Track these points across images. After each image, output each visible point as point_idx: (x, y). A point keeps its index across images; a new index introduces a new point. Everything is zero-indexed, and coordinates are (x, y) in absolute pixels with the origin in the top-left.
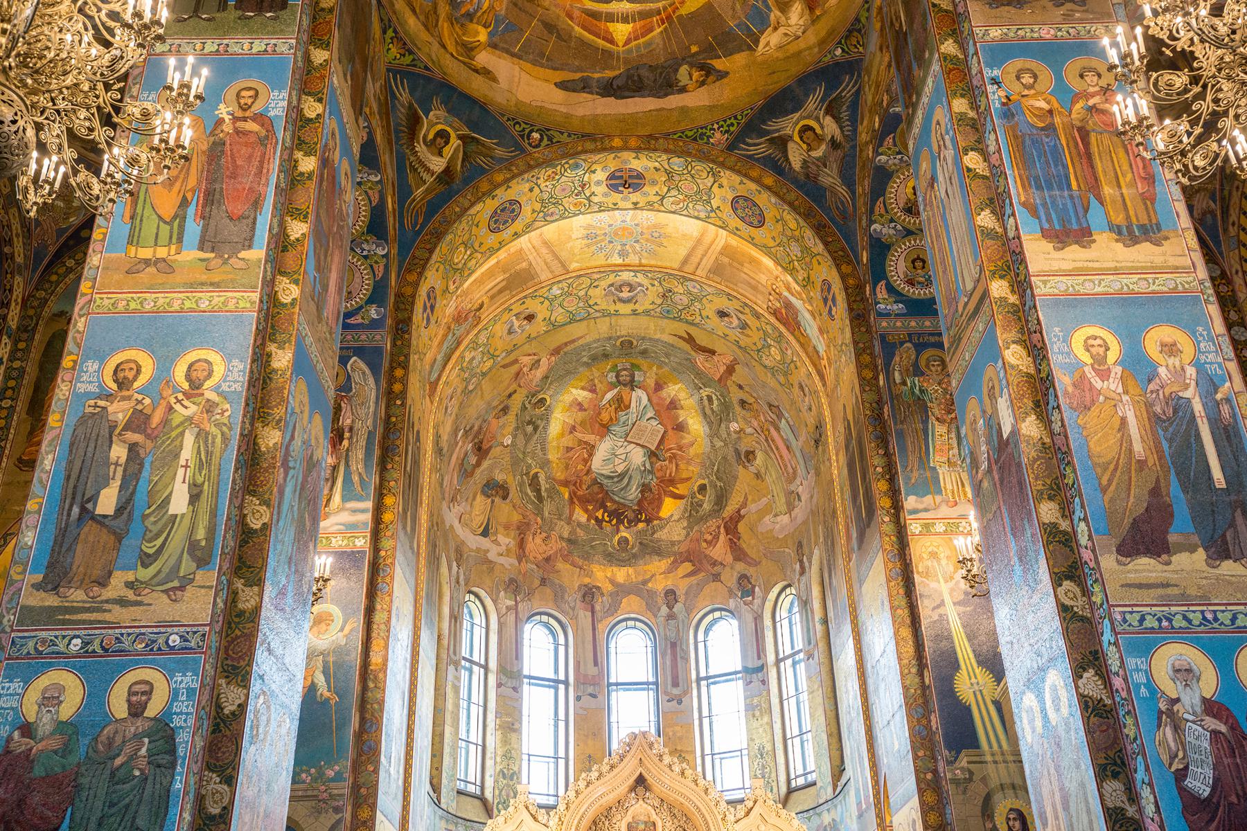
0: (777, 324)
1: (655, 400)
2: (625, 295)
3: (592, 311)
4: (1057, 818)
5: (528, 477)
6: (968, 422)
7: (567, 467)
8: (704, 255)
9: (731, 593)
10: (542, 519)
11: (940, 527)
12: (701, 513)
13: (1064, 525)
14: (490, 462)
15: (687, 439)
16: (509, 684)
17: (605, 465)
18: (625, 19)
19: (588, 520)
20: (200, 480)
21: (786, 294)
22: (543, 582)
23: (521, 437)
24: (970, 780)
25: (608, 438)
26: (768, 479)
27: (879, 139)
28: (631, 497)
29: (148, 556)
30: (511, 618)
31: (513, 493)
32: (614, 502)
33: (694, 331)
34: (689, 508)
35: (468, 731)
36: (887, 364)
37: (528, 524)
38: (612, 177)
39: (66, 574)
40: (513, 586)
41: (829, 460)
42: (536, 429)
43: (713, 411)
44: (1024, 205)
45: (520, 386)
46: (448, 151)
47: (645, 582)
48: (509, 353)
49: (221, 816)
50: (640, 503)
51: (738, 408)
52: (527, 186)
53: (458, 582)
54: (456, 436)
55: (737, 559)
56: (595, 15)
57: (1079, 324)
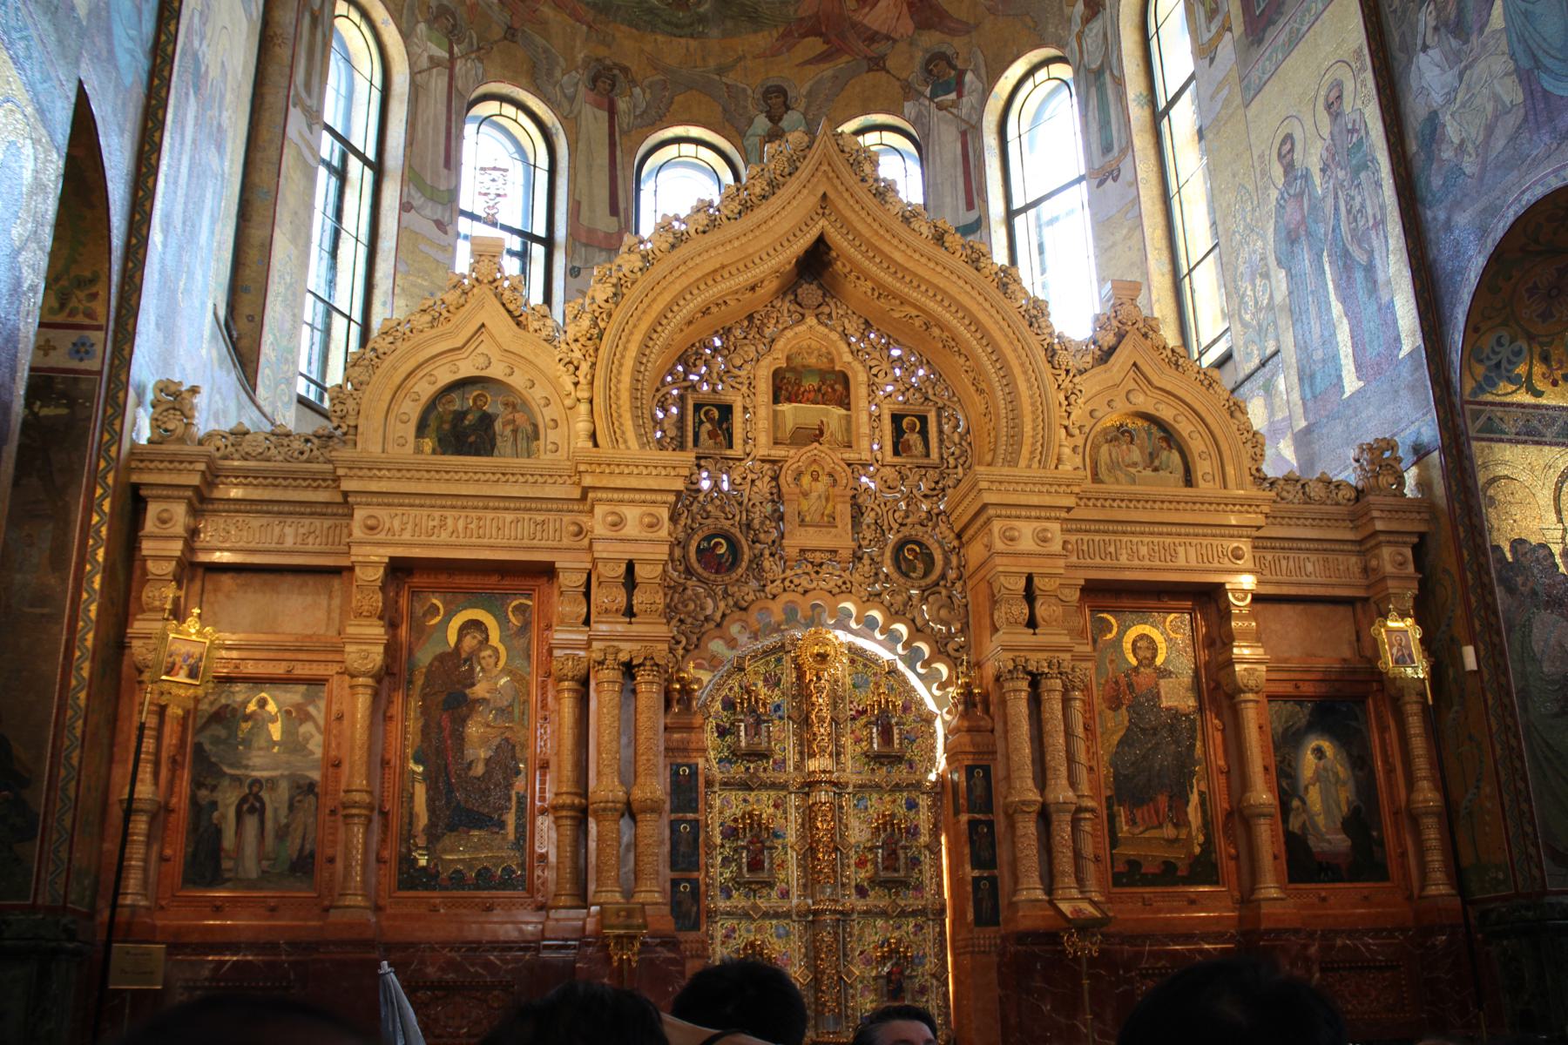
9: (909, 92)
16: (428, 212)
35: (332, 283)
40: (448, 24)
55: (923, 25)
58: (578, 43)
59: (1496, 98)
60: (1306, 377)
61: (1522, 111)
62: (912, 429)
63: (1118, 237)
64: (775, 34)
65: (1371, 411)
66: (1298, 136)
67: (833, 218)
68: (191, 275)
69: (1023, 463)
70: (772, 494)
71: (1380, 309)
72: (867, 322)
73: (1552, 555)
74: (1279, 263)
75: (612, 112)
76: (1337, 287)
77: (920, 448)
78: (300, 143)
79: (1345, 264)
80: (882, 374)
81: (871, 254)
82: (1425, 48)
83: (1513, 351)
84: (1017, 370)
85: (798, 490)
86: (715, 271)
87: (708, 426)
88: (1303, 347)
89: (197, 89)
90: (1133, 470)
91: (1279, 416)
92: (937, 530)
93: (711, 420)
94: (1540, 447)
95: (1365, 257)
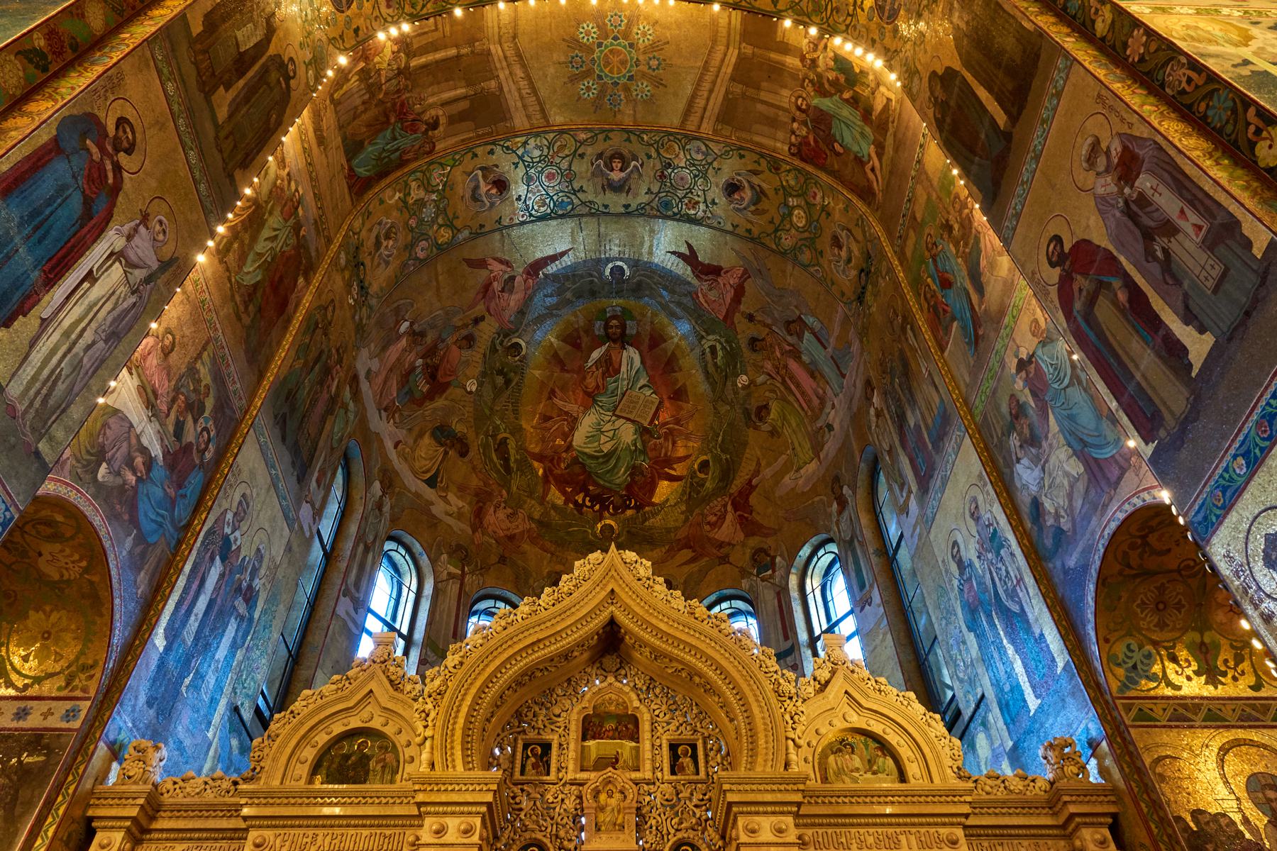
0: (802, 165)
1: (649, 362)
2: (616, 176)
3: (576, 201)
5: (495, 440)
7: (543, 440)
8: (711, 91)
9: (744, 573)
10: (508, 493)
12: (703, 493)
14: (446, 403)
17: (589, 443)
19: (566, 503)
21: (816, 101)
22: (502, 560)
23: (487, 390)
25: (593, 410)
26: (787, 432)
28: (618, 481)
30: (453, 588)
32: (596, 484)
34: (688, 490)
37: (490, 494)
40: (462, 554)
41: (891, 270)
42: (508, 382)
43: (715, 364)
45: (488, 311)
50: (629, 487)
51: (746, 352)
53: (379, 506)
54: (398, 323)
58: (545, 563)
59: (1067, 474)
60: (1004, 707)
61: (1086, 476)
62: (685, 755)
63: (878, 641)
64: (664, 550)
65: (1051, 721)
66: (960, 541)
67: (619, 605)
68: (200, 676)
69: (759, 769)
70: (576, 809)
71: (1036, 640)
72: (651, 679)
73: (1233, 823)
74: (970, 629)
76: (1006, 634)
77: (692, 768)
78: (346, 618)
79: (1007, 615)
80: (662, 715)
81: (644, 627)
82: (1018, 460)
83: (1143, 656)
84: (751, 699)
85: (595, 805)
86: (533, 644)
87: (533, 760)
88: (996, 684)
89: (223, 560)
90: (856, 775)
91: (996, 745)
92: (706, 833)
93: (535, 755)
94: (1193, 730)
95: (1017, 607)
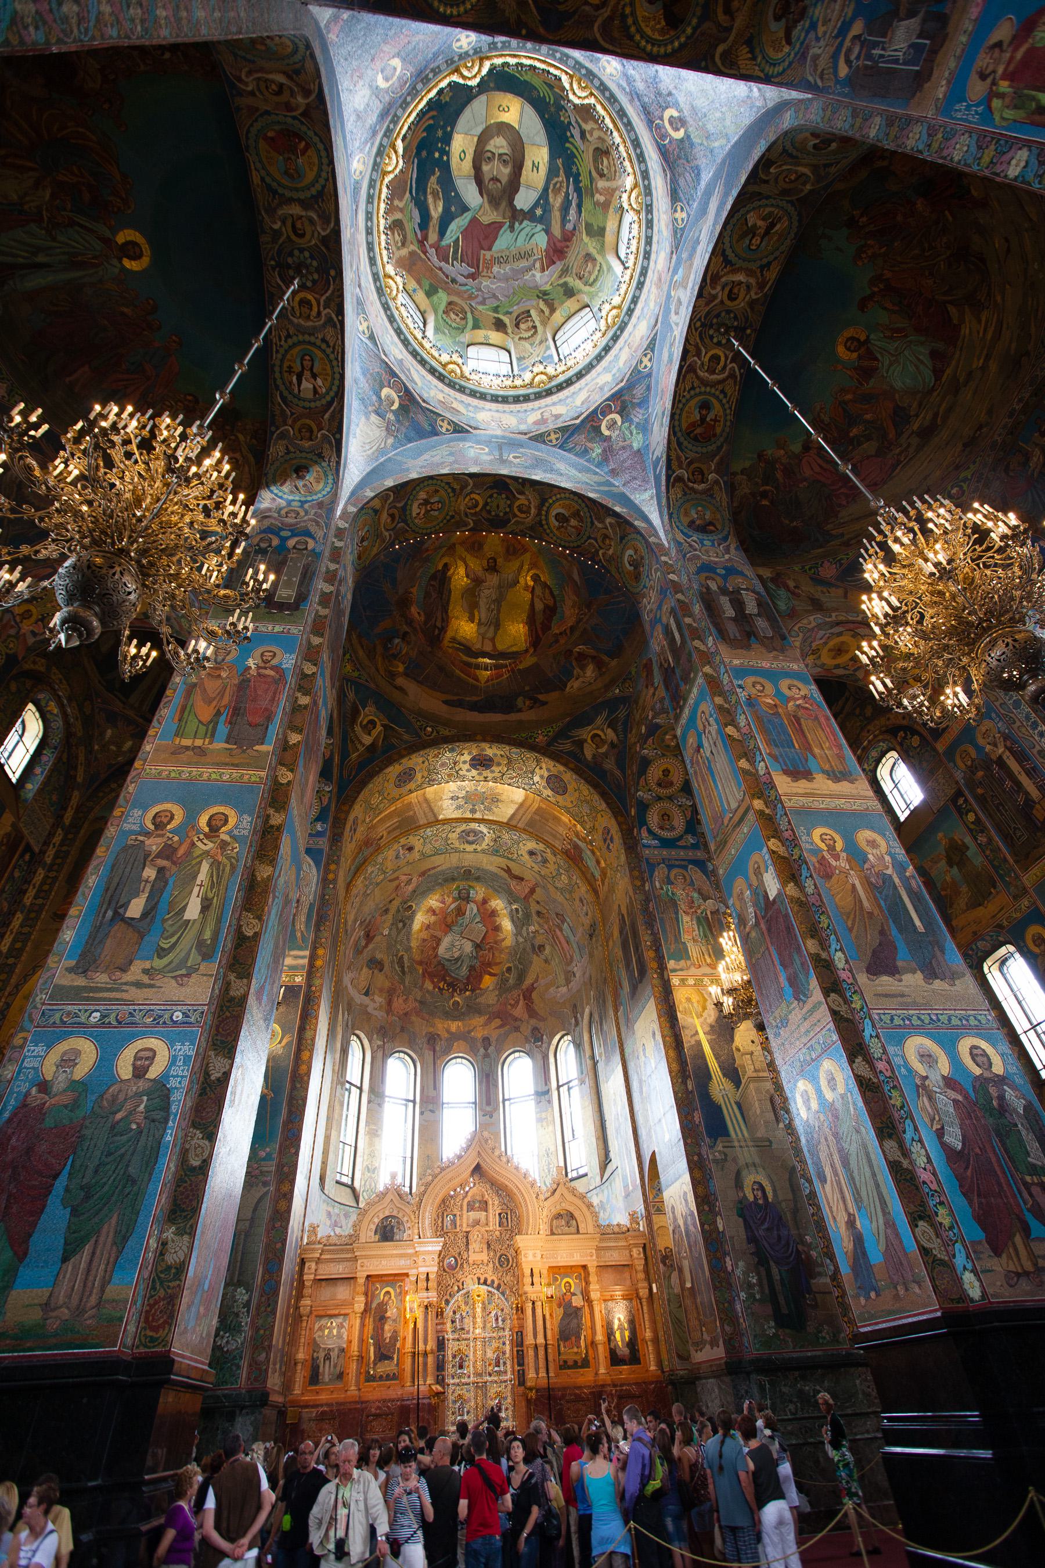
2: (470, 839)
4: (836, 1174)
6: (735, 895)
9: (527, 1040)
11: (691, 982)
13: (824, 955)
15: (501, 936)
18: (486, 669)
20: (210, 895)
22: (402, 1029)
24: (726, 1160)
27: (644, 739)
29: (163, 949)
30: (380, 1054)
31: (387, 967)
33: (511, 865)
36: (651, 876)
38: (472, 759)
39: (95, 961)
44: (769, 754)
46: (375, 733)
47: (469, 1032)
48: (394, 871)
49: (201, 1167)
50: (468, 978)
51: (535, 917)
52: (421, 760)
55: (531, 1016)
56: (469, 665)
57: (814, 827)
75: (434, 1051)
